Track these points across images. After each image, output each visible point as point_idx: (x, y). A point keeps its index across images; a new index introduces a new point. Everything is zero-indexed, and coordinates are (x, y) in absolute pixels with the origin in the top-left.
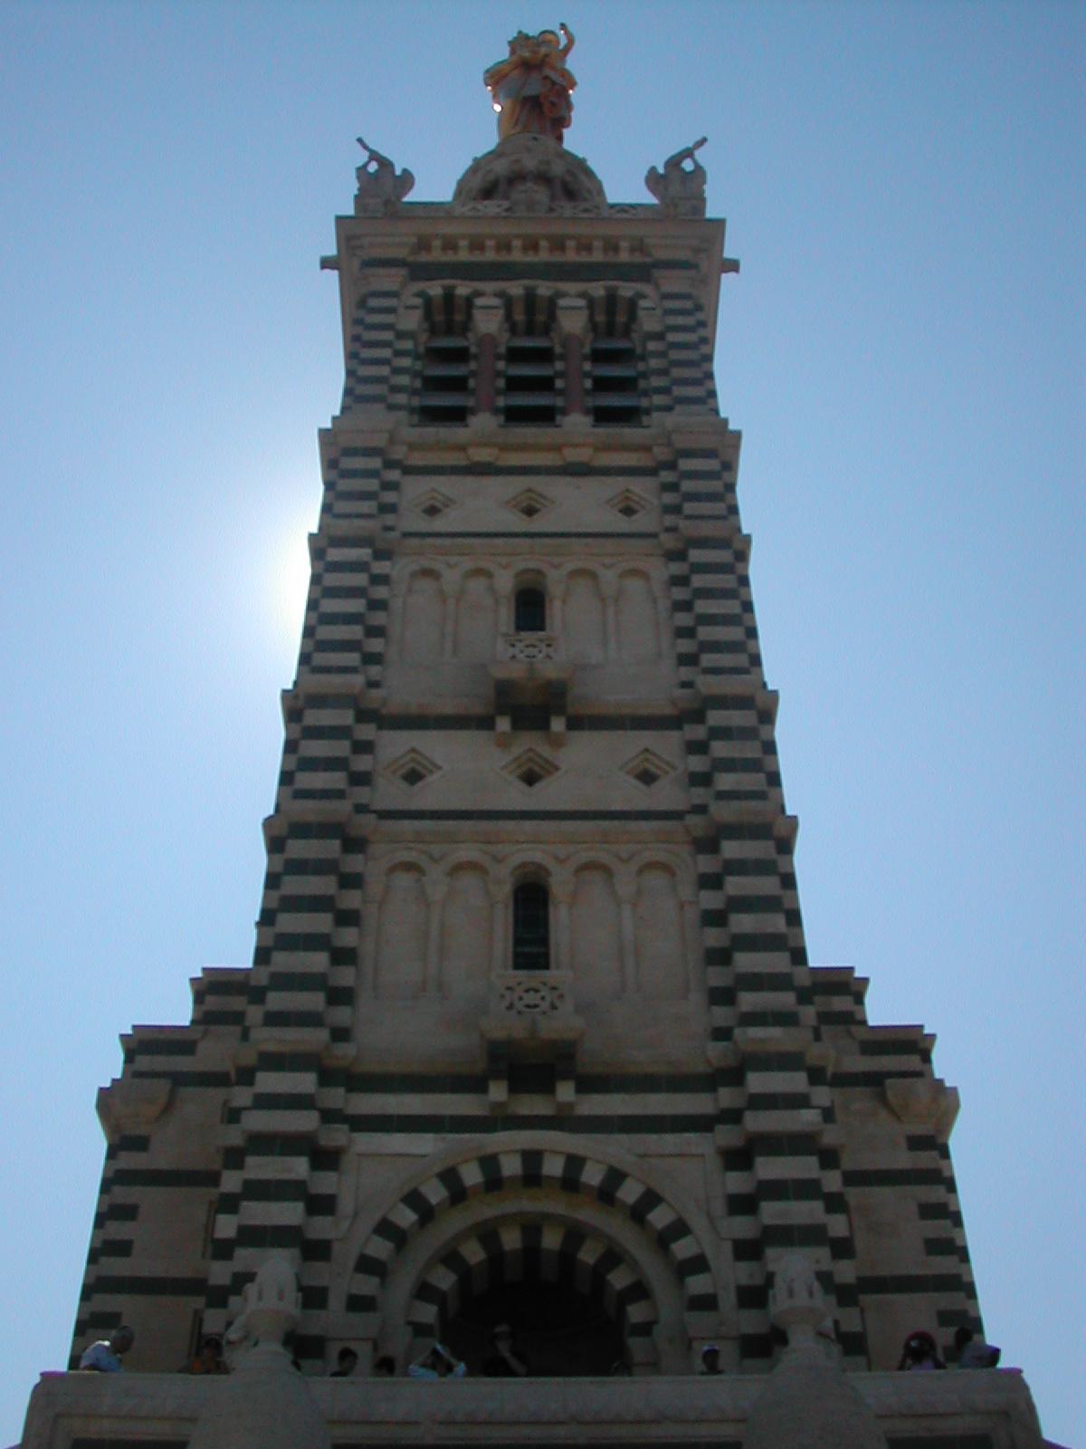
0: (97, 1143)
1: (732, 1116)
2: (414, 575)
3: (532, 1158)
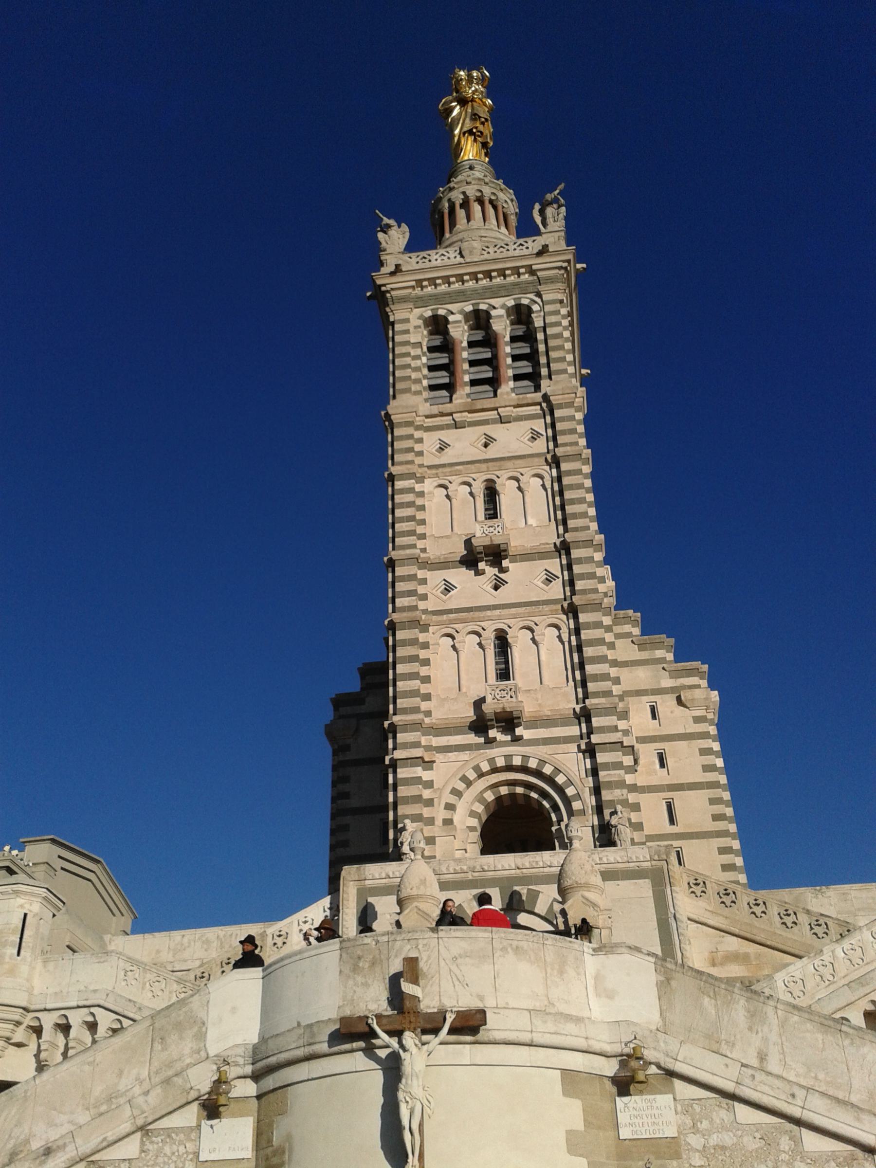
0: (327, 750)
3: (508, 757)
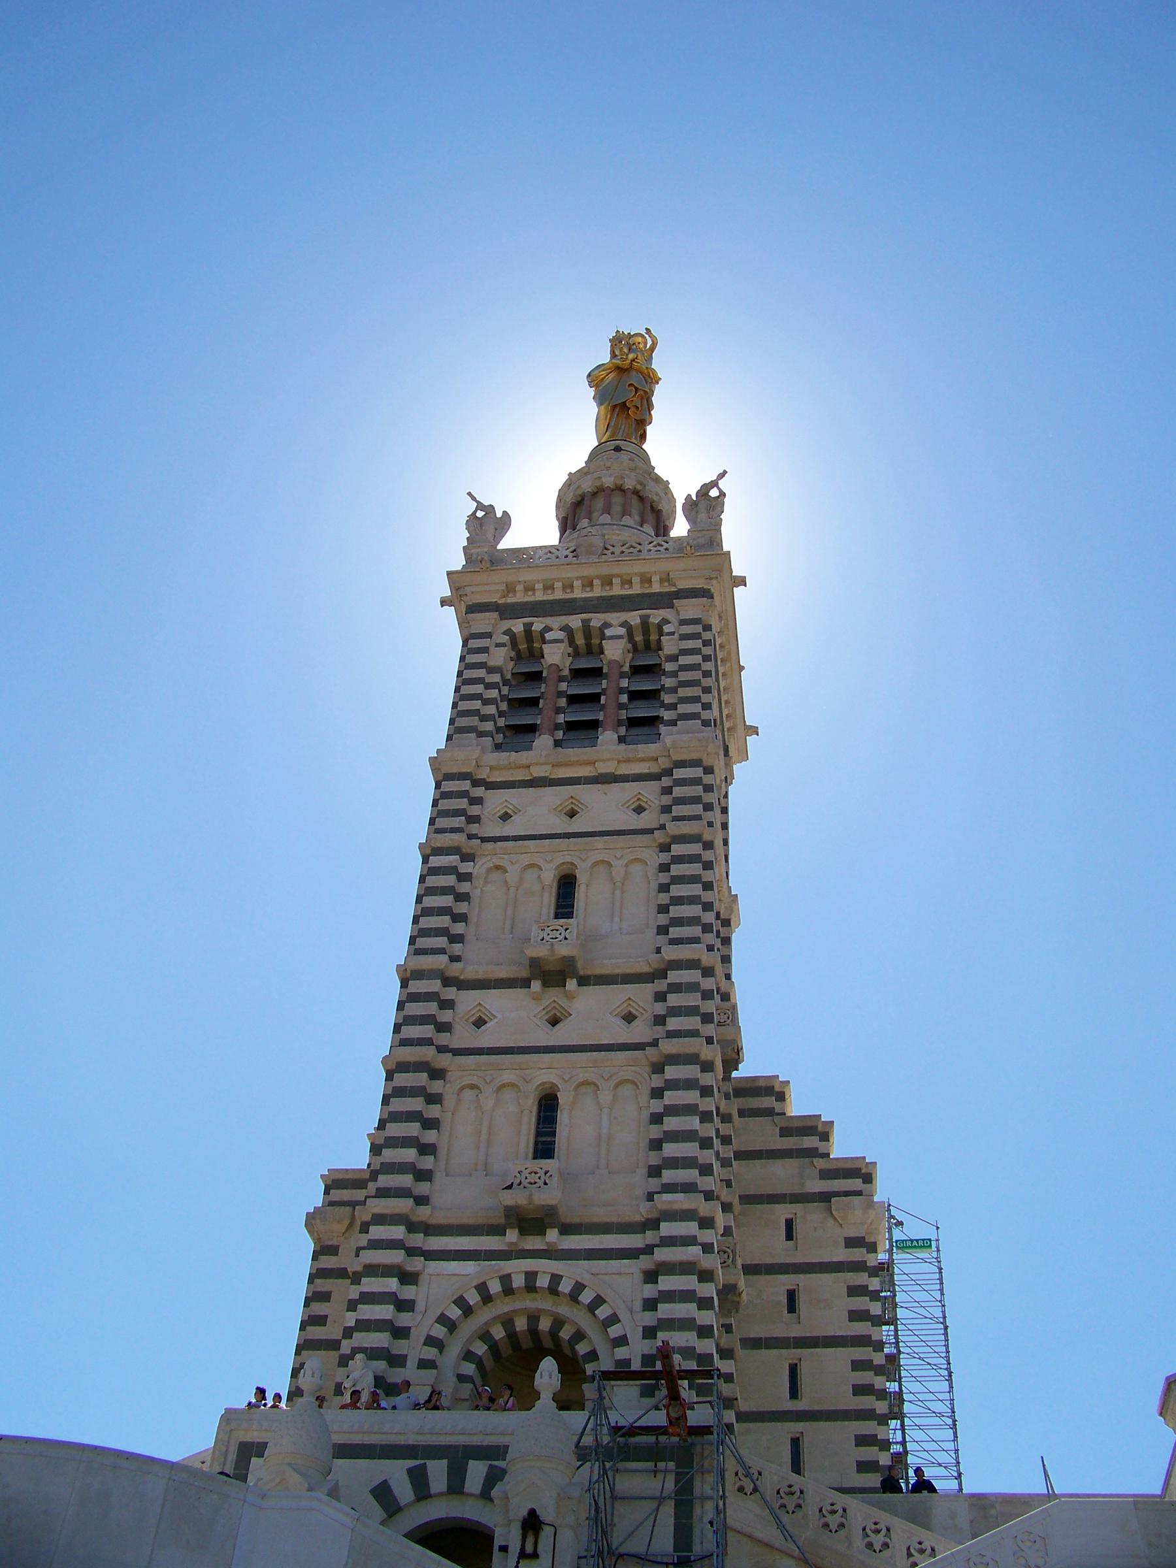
1: (649, 1250)
2: (490, 870)
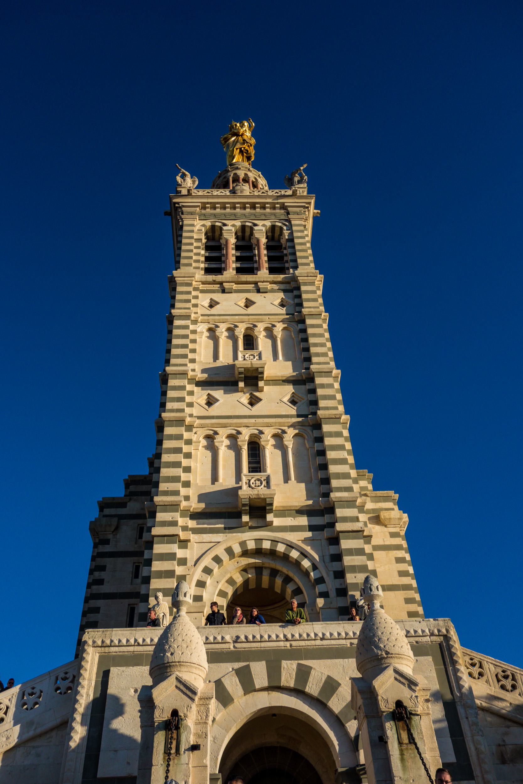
0: (89, 542)
3: (259, 541)
